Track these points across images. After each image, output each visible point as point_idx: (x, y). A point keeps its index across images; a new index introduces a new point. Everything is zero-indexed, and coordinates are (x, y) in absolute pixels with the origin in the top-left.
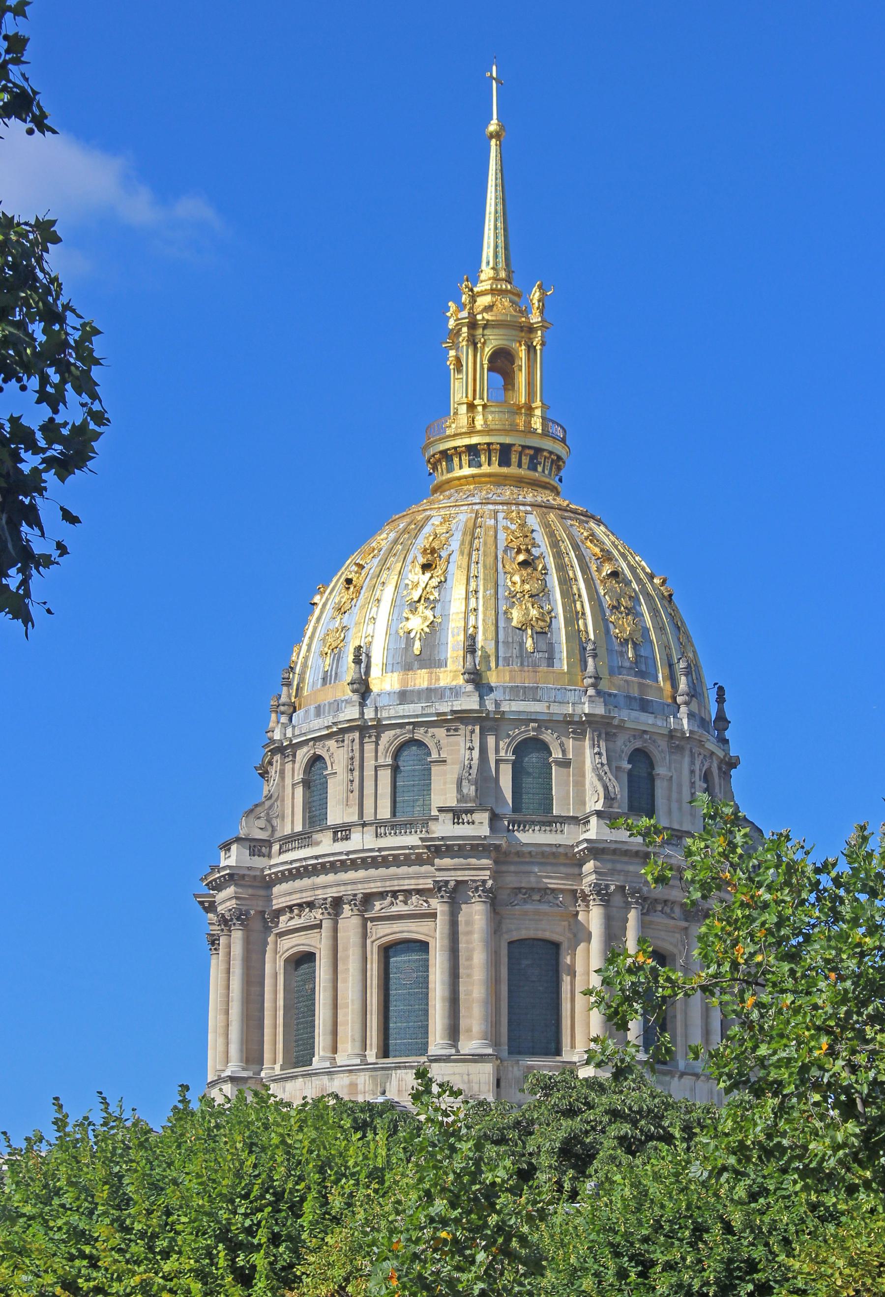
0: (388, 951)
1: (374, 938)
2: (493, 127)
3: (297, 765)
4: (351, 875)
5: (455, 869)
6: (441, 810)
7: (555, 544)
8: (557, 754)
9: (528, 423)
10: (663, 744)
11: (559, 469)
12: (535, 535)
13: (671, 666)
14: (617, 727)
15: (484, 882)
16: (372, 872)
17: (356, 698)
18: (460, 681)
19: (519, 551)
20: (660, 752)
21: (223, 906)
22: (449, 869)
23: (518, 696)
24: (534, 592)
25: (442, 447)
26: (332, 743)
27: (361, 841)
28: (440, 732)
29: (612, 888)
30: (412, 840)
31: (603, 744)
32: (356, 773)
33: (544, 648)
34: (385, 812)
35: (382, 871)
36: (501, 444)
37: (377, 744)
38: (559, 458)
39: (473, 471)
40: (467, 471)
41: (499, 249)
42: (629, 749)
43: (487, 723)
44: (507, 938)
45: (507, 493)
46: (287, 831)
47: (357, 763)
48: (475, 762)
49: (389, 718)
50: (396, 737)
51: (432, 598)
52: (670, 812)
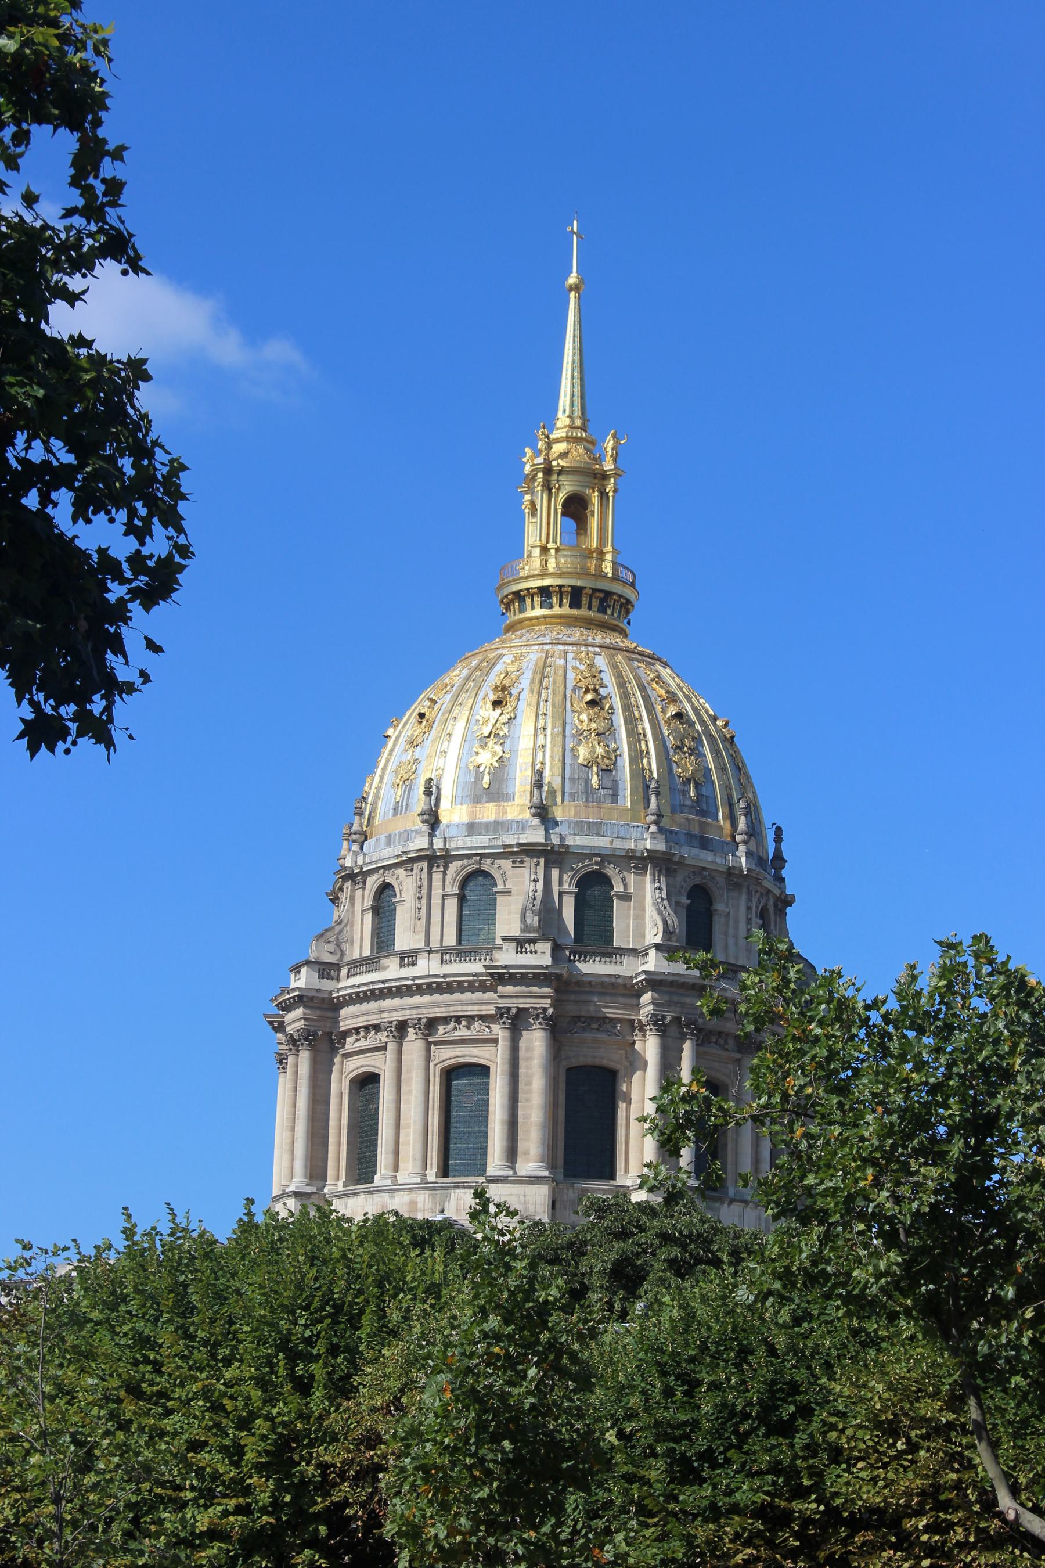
0: (451, 1074)
1: (437, 1061)
2: (572, 280)
3: (367, 892)
4: (417, 1000)
5: (517, 997)
6: (505, 939)
7: (622, 685)
8: (618, 888)
9: (599, 567)
10: (721, 880)
11: (628, 612)
12: (602, 675)
13: (731, 806)
14: (678, 863)
15: (545, 1010)
16: (437, 997)
17: (425, 828)
18: (527, 814)
19: (587, 691)
21: (292, 1026)
22: (512, 997)
23: (582, 831)
24: (601, 730)
25: (515, 588)
26: (401, 872)
27: (427, 967)
29: (669, 1018)
30: (476, 967)
31: (663, 879)
32: (424, 901)
34: (451, 940)
35: (446, 997)
36: (572, 587)
37: (445, 874)
38: (628, 602)
39: (545, 612)
40: (539, 612)
41: (576, 398)
42: (688, 886)
43: (552, 856)
44: (565, 1064)
45: (577, 634)
46: (356, 956)
47: (425, 891)
48: (539, 894)
49: (457, 849)
51: (501, 733)
52: (726, 947)
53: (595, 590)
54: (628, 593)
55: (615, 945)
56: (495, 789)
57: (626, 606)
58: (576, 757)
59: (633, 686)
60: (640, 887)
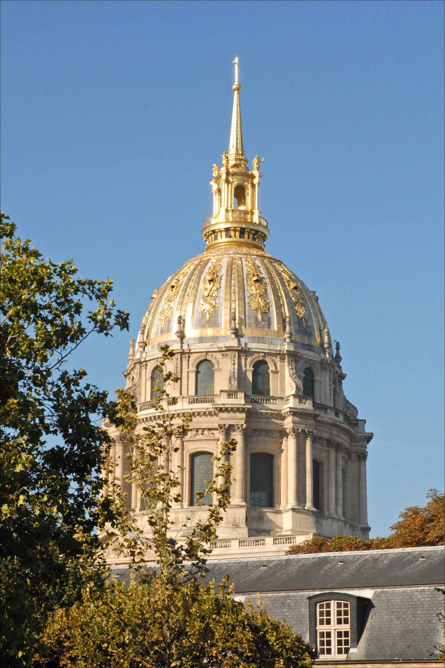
0: (193, 456)
1: (187, 450)
3: (148, 370)
5: (228, 419)
7: (269, 273)
8: (271, 368)
9: (252, 219)
10: (318, 366)
11: (264, 241)
12: (260, 269)
13: (320, 331)
14: (300, 357)
15: (242, 425)
17: (178, 339)
18: (229, 332)
19: (254, 275)
20: (317, 369)
22: (226, 419)
23: (255, 340)
24: (262, 294)
25: (213, 228)
28: (219, 355)
29: (300, 430)
31: (293, 364)
33: (266, 320)
34: (192, 392)
37: (189, 361)
38: (265, 236)
41: (238, 141)
42: (304, 368)
44: (249, 452)
45: (245, 250)
46: (143, 400)
48: (236, 371)
50: (198, 358)
51: (214, 295)
52: (320, 398)
53: (251, 230)
54: (265, 231)
55: (271, 395)
56: (212, 321)
57: (264, 237)
58: (250, 306)
59: (274, 273)
60: (283, 368)
